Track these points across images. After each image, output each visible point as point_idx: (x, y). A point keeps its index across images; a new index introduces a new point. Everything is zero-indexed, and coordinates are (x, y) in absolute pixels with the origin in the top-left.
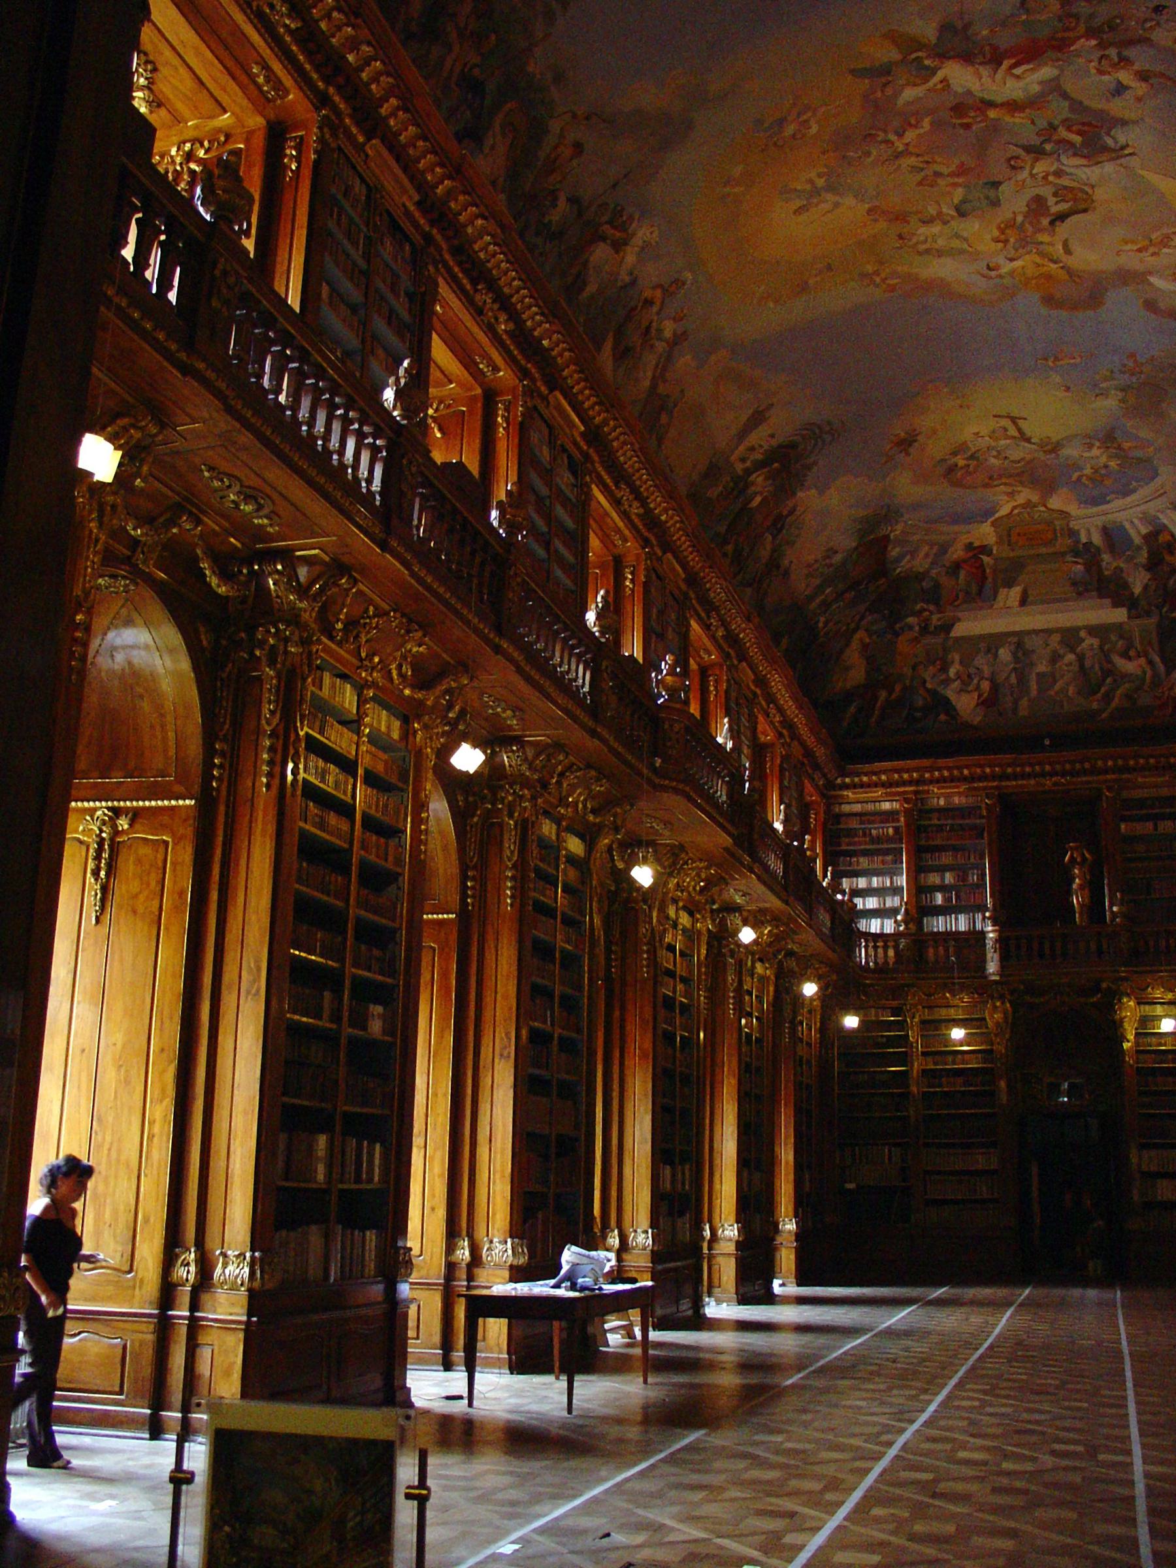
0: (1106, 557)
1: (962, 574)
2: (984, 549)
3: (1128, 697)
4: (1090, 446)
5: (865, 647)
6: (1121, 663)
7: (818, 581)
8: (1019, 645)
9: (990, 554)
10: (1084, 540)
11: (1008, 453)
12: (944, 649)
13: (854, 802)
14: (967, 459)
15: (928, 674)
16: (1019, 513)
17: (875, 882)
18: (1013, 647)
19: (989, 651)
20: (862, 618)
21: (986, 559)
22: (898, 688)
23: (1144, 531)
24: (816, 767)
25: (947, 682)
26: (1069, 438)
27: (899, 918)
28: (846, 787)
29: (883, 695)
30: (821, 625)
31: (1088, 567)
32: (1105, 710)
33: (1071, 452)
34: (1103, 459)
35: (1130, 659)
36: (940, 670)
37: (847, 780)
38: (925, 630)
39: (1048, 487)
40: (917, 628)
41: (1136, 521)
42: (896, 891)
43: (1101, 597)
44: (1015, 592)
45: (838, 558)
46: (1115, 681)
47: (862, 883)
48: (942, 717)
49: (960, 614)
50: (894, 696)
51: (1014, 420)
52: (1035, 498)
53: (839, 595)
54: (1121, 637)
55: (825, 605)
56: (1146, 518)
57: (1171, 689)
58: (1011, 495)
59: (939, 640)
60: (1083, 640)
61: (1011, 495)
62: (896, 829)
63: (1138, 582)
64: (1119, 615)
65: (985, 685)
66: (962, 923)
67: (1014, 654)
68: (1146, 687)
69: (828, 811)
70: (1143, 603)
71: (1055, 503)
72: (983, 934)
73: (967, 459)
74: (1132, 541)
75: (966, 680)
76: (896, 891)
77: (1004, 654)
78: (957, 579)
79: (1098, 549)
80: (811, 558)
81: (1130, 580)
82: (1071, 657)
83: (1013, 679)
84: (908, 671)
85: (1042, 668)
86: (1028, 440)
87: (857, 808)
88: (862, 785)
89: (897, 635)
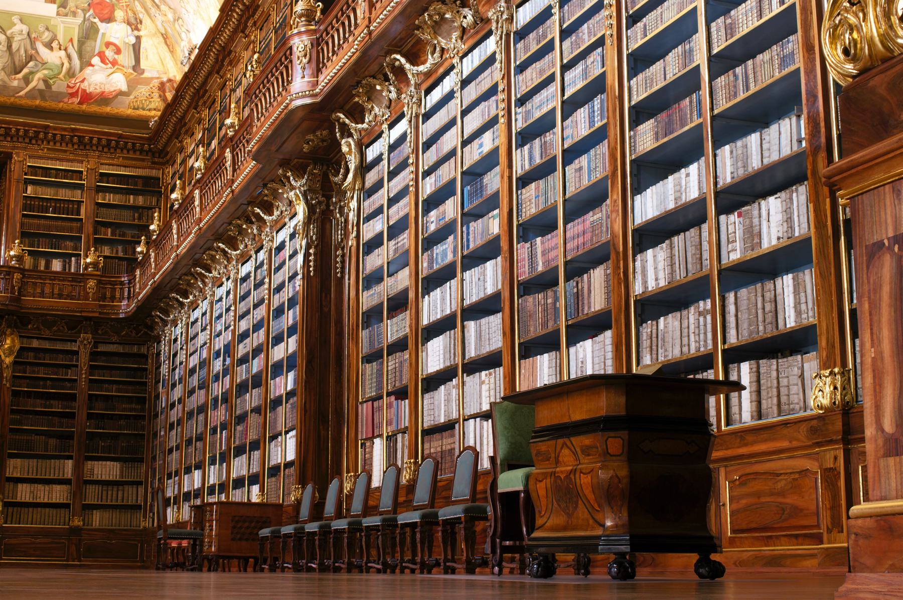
6: (43, 51)
32: (23, 89)
35: (51, 49)
46: (36, 65)
54: (47, 29)
57: (83, 81)
68: (61, 76)
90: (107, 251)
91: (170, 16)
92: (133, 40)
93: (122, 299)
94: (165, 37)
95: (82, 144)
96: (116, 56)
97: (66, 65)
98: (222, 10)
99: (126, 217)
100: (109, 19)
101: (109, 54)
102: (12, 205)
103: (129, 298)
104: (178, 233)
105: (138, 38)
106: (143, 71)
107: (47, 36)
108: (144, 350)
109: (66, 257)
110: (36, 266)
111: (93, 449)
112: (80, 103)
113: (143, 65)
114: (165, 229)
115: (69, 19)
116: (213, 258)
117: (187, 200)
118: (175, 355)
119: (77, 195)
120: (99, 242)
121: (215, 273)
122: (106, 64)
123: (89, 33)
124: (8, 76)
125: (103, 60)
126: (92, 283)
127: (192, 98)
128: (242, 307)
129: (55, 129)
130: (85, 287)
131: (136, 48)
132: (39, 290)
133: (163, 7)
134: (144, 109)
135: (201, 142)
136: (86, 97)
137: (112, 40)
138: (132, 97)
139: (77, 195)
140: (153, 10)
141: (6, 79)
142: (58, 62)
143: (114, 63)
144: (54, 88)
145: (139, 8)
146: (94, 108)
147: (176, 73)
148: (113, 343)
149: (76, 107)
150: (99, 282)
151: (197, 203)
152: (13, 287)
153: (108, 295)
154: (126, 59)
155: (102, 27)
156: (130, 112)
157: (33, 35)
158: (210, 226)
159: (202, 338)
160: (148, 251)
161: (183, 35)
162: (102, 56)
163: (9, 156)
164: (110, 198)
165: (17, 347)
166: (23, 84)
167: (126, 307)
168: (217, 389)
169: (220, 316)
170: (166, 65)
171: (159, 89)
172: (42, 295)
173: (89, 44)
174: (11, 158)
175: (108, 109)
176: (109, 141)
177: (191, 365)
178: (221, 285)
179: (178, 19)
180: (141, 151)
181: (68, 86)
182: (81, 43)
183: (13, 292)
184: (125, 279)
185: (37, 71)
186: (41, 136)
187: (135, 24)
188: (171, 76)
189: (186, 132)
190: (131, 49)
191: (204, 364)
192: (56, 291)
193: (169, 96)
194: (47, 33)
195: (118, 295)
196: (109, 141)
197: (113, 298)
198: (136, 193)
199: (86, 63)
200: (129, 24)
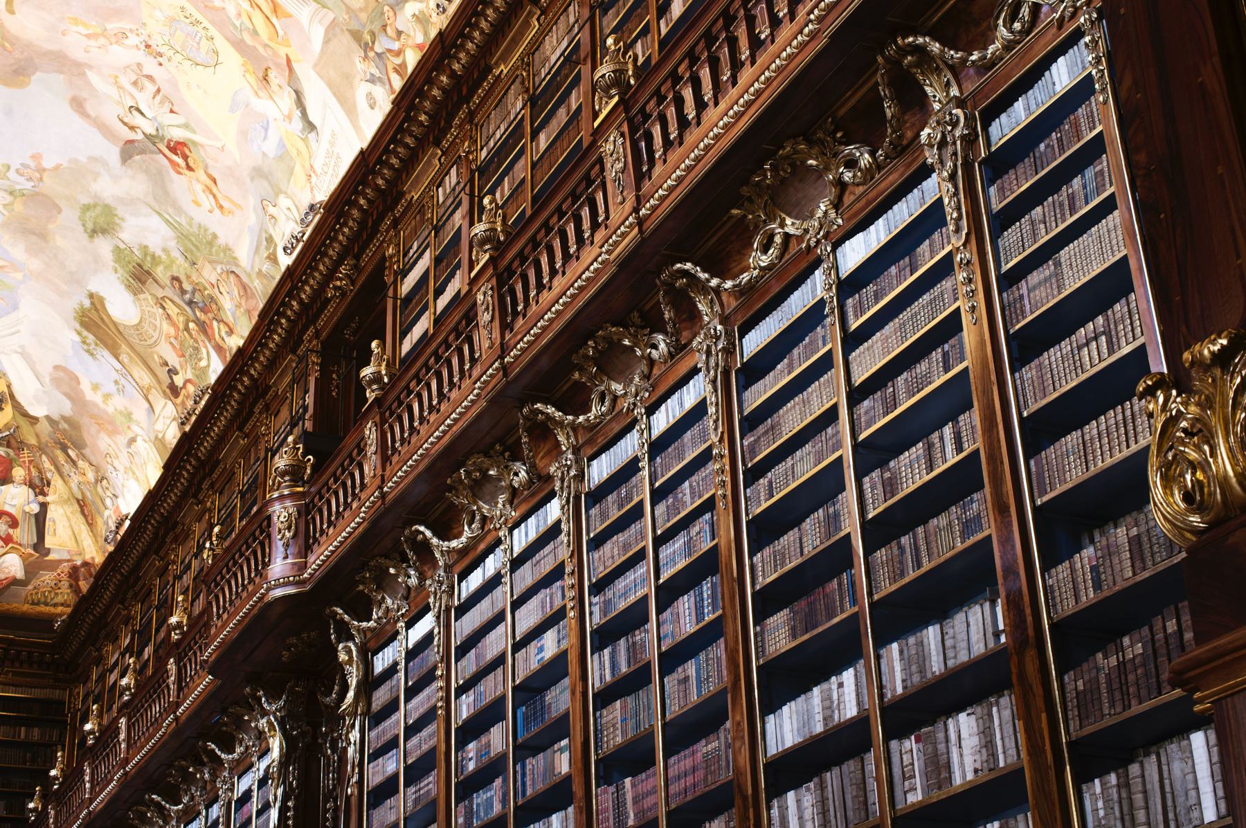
91: (91, 476)
92: (35, 508)
94: (82, 505)
96: (11, 531)
98: (167, 467)
104: (92, 781)
105: (44, 506)
106: (48, 551)
113: (49, 542)
114: (72, 776)
117: (108, 733)
131: (40, 520)
133: (81, 463)
134: (46, 604)
135: (129, 650)
137: (8, 509)
138: (30, 587)
140: (67, 468)
145: (47, 464)
147: (94, 552)
151: (122, 736)
154: (24, 534)
156: (26, 607)
158: (142, 768)
160: (45, 807)
161: (108, 502)
170: (78, 542)
171: (70, 576)
179: (100, 479)
187: (39, 486)
188: (88, 557)
190: (33, 520)
193: (84, 586)
198: (29, 723)
200: (32, 486)
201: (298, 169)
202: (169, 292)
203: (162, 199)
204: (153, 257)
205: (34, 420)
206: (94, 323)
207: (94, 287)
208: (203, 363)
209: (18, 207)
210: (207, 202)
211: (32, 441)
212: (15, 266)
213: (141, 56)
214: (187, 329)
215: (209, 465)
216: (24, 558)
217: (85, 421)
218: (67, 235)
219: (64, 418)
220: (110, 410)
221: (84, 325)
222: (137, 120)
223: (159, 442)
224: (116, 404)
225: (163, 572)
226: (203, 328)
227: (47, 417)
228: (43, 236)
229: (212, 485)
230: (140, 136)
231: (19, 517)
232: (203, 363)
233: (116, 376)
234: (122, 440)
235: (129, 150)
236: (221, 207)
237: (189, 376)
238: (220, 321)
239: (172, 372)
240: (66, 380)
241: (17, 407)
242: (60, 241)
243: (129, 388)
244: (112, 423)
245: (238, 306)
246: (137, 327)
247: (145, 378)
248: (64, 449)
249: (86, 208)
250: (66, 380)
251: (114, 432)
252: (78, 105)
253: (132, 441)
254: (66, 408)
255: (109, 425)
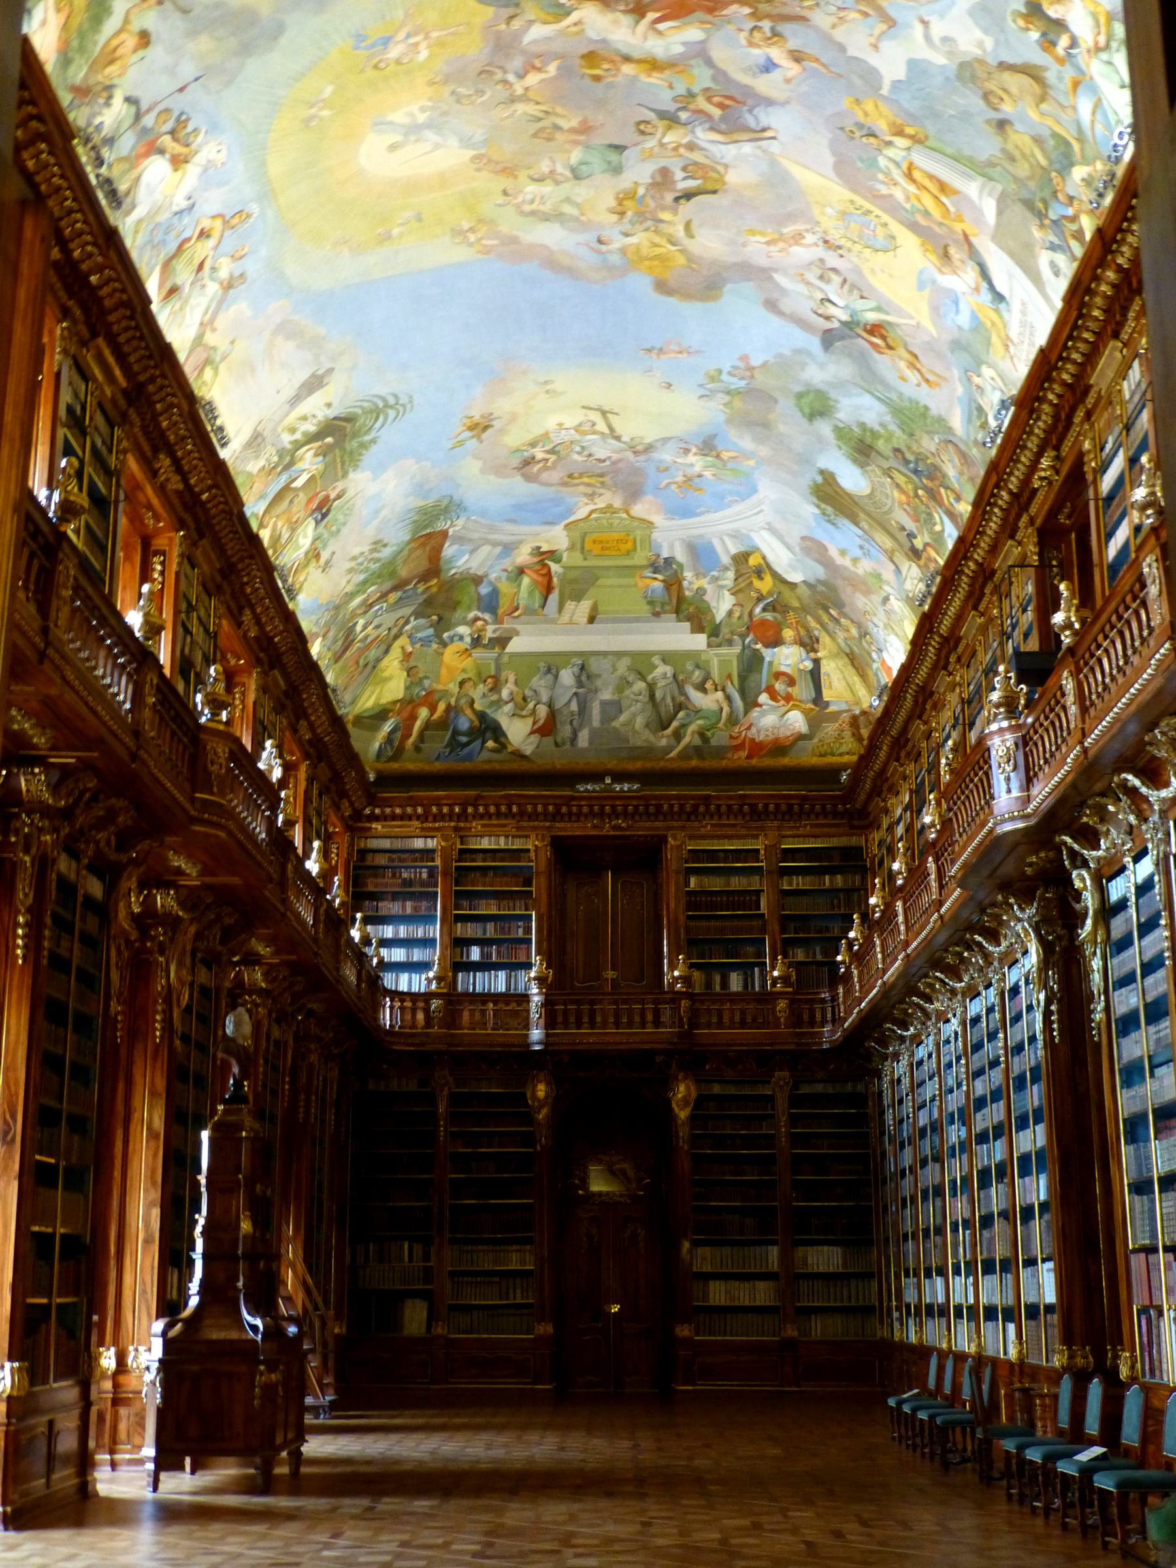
0: (688, 574)
1: (526, 581)
2: (552, 554)
3: (701, 734)
4: (687, 451)
5: (407, 656)
6: (695, 696)
7: (362, 577)
8: (583, 668)
9: (558, 561)
10: (665, 555)
11: (594, 450)
12: (498, 668)
13: (382, 837)
14: (548, 452)
15: (477, 692)
16: (596, 519)
17: (403, 931)
18: (576, 669)
19: (549, 670)
20: (407, 622)
21: (555, 567)
22: (441, 707)
23: (733, 551)
24: (343, 794)
25: (499, 703)
26: (665, 440)
27: (431, 974)
28: (377, 819)
29: (424, 713)
30: (359, 628)
31: (668, 585)
33: (666, 456)
34: (697, 469)
35: (705, 691)
36: (491, 690)
37: (377, 811)
38: (476, 642)
39: (634, 493)
40: (468, 640)
41: (726, 539)
42: (427, 942)
43: (679, 620)
44: (585, 606)
45: (386, 553)
46: (687, 715)
47: (388, 932)
48: (490, 744)
49: (518, 627)
50: (435, 716)
51: (604, 413)
52: (617, 503)
53: (384, 596)
54: (698, 667)
55: (368, 606)
56: (736, 535)
57: (749, 728)
58: (591, 497)
59: (493, 654)
60: (656, 667)
61: (591, 497)
62: (432, 872)
63: (722, 605)
64: (700, 641)
65: (543, 711)
66: (499, 982)
67: (578, 679)
69: (352, 844)
70: (725, 631)
71: (638, 510)
72: (525, 998)
73: (548, 452)
74: (718, 558)
75: (520, 704)
76: (427, 942)
77: (567, 677)
78: (519, 586)
79: (681, 566)
80: (356, 551)
81: (713, 604)
82: (640, 685)
83: (574, 706)
84: (453, 688)
85: (606, 695)
86: (618, 438)
87: (386, 844)
88: (394, 817)
89: (444, 645)
90: (800, 955)
91: (854, 632)
92: (809, 665)
93: (823, 1023)
95: (755, 815)
97: (726, 709)
99: (821, 907)
100: (776, 642)
101: (779, 686)
102: (672, 905)
103: (834, 1021)
104: (883, 952)
105: (817, 662)
106: (827, 704)
107: (697, 675)
108: (860, 1087)
109: (746, 969)
110: (709, 984)
111: (805, 1229)
112: (749, 757)
113: (827, 695)
114: (868, 944)
115: (723, 650)
116: (932, 986)
118: (901, 1102)
119: (754, 883)
120: (785, 948)
121: (937, 1005)
122: (776, 700)
123: (751, 663)
124: (655, 732)
125: (774, 696)
126: (782, 1004)
127: (891, 748)
128: (977, 1060)
129: (718, 798)
130: (774, 1010)
131: (815, 675)
132: (715, 1020)
134: (833, 754)
136: (756, 748)
137: (783, 669)
138: (816, 740)
139: (754, 883)
140: (831, 625)
141: (652, 738)
142: (715, 707)
143: (788, 698)
144: (713, 742)
145: (813, 624)
146: (768, 762)
148: (819, 1082)
149: (744, 763)
150: (793, 1003)
151: (901, 918)
152: (681, 1019)
153: (806, 1017)
154: (803, 691)
155: (767, 653)
156: (815, 761)
157: (681, 678)
159: (930, 1089)
161: (874, 655)
162: (771, 691)
163: (664, 839)
164: (799, 883)
165: (694, 1094)
166: (673, 741)
167: (829, 1035)
168: (956, 1169)
169: (949, 1065)
170: (852, 693)
172: (720, 1025)
173: (753, 678)
174: (666, 842)
175: (786, 761)
176: (790, 806)
177: (921, 1123)
178: (948, 1021)
179: (864, 634)
180: (835, 814)
181: (731, 737)
182: (743, 679)
183: (681, 1026)
184: (826, 995)
185: (691, 723)
186: (702, 809)
187: (809, 644)
188: (865, 706)
189: (890, 790)
191: (936, 1127)
192: (737, 1018)
194: (697, 673)
195: (818, 1016)
196: (790, 806)
197: (812, 1023)
198: (832, 871)
199: (751, 703)
200: (802, 644)
201: (995, 339)
202: (892, 463)
203: (870, 380)
204: (872, 431)
205: (793, 586)
206: (828, 493)
207: (824, 462)
208: (938, 528)
209: (737, 403)
210: (913, 377)
211: (796, 604)
212: (747, 456)
213: (820, 252)
214: (917, 496)
215: (951, 641)
216: (805, 713)
217: (840, 583)
218: (788, 421)
219: (818, 581)
220: (860, 572)
221: (820, 498)
222: (831, 310)
223: (909, 600)
224: (864, 567)
225: (928, 737)
226: (933, 495)
227: (804, 582)
228: (766, 425)
229: (959, 659)
230: (836, 325)
231: (796, 675)
232: (938, 528)
233: (859, 542)
234: (877, 599)
235: (829, 339)
236: (927, 381)
237: (927, 539)
238: (947, 488)
239: (911, 536)
240: (814, 549)
241: (775, 575)
242: (782, 428)
243: (873, 552)
244: (864, 583)
245: (961, 473)
246: (871, 496)
247: (889, 543)
248: (826, 609)
249: (800, 396)
250: (814, 549)
251: (868, 592)
252: (772, 305)
253: (886, 599)
254: (820, 572)
255: (864, 586)
